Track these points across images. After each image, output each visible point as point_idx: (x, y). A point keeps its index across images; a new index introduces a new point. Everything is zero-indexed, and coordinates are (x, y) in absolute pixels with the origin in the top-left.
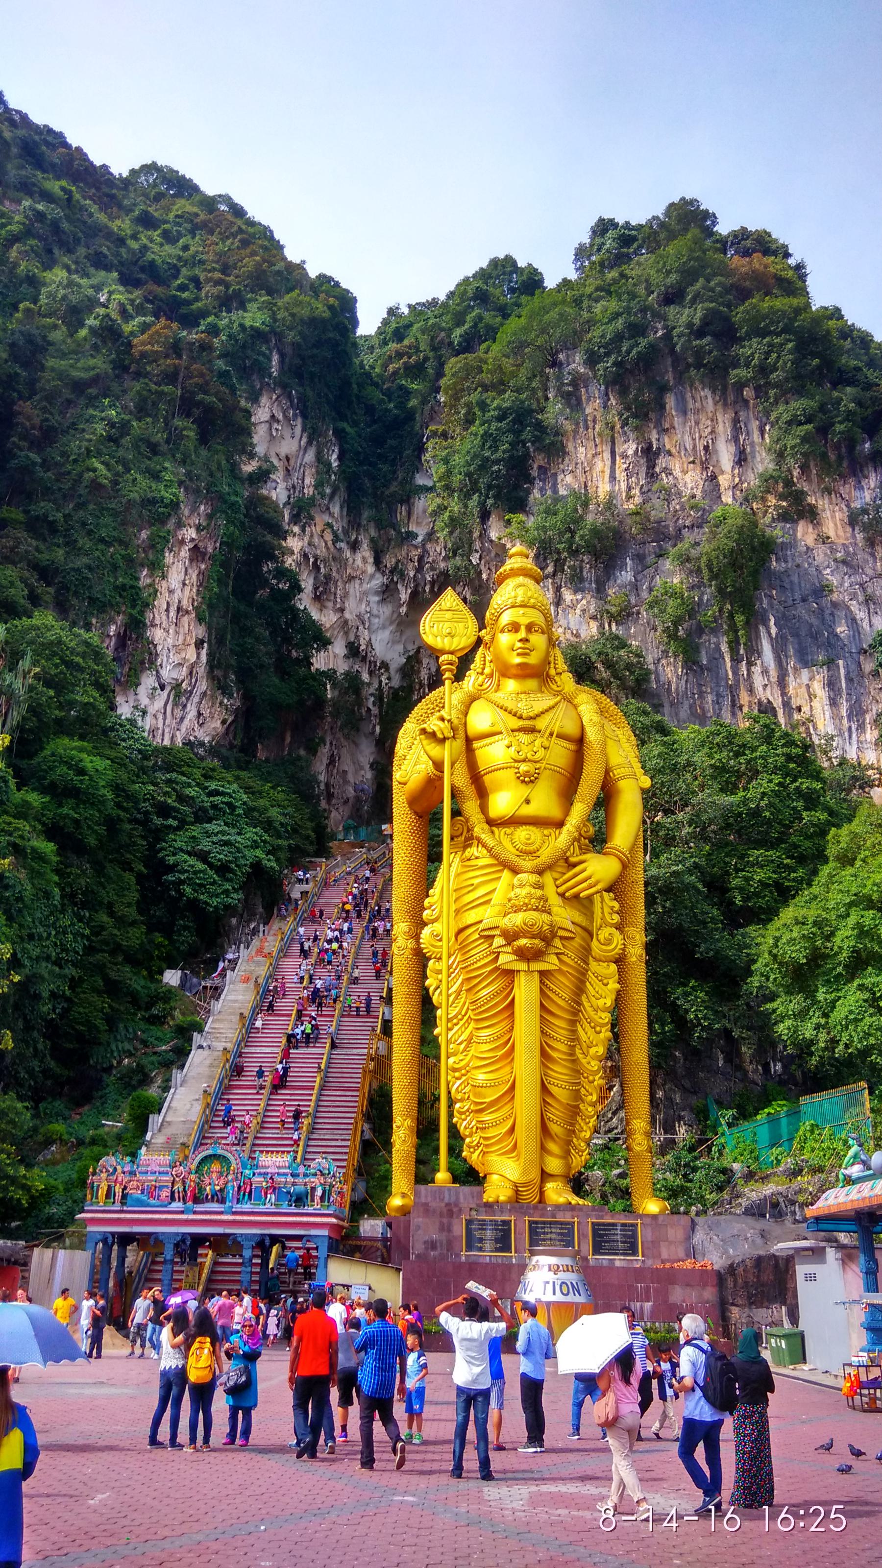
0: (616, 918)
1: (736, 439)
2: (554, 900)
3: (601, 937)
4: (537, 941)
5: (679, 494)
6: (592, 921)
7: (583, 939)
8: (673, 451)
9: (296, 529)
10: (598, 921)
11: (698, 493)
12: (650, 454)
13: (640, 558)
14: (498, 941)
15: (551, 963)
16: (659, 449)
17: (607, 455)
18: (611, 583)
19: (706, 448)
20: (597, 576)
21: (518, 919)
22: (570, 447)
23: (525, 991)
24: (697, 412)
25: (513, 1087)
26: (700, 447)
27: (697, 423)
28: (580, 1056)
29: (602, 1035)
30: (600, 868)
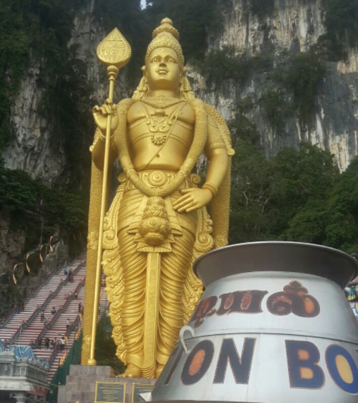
0: (210, 228)
1: (308, 20)
2: (171, 212)
3: (201, 239)
4: (157, 234)
5: (280, 48)
6: (196, 226)
7: (187, 236)
8: (277, 27)
9: (102, 86)
10: (200, 229)
11: (289, 47)
12: (265, 29)
13: (258, 80)
14: (138, 235)
15: (167, 248)
16: (270, 26)
17: (244, 31)
18: (243, 94)
19: (294, 25)
20: (236, 90)
21: (148, 223)
22: (226, 27)
23: (153, 263)
24: (290, 7)
25: (143, 318)
26: (291, 25)
27: (290, 13)
28: (185, 303)
29: (198, 292)
30: (198, 197)
